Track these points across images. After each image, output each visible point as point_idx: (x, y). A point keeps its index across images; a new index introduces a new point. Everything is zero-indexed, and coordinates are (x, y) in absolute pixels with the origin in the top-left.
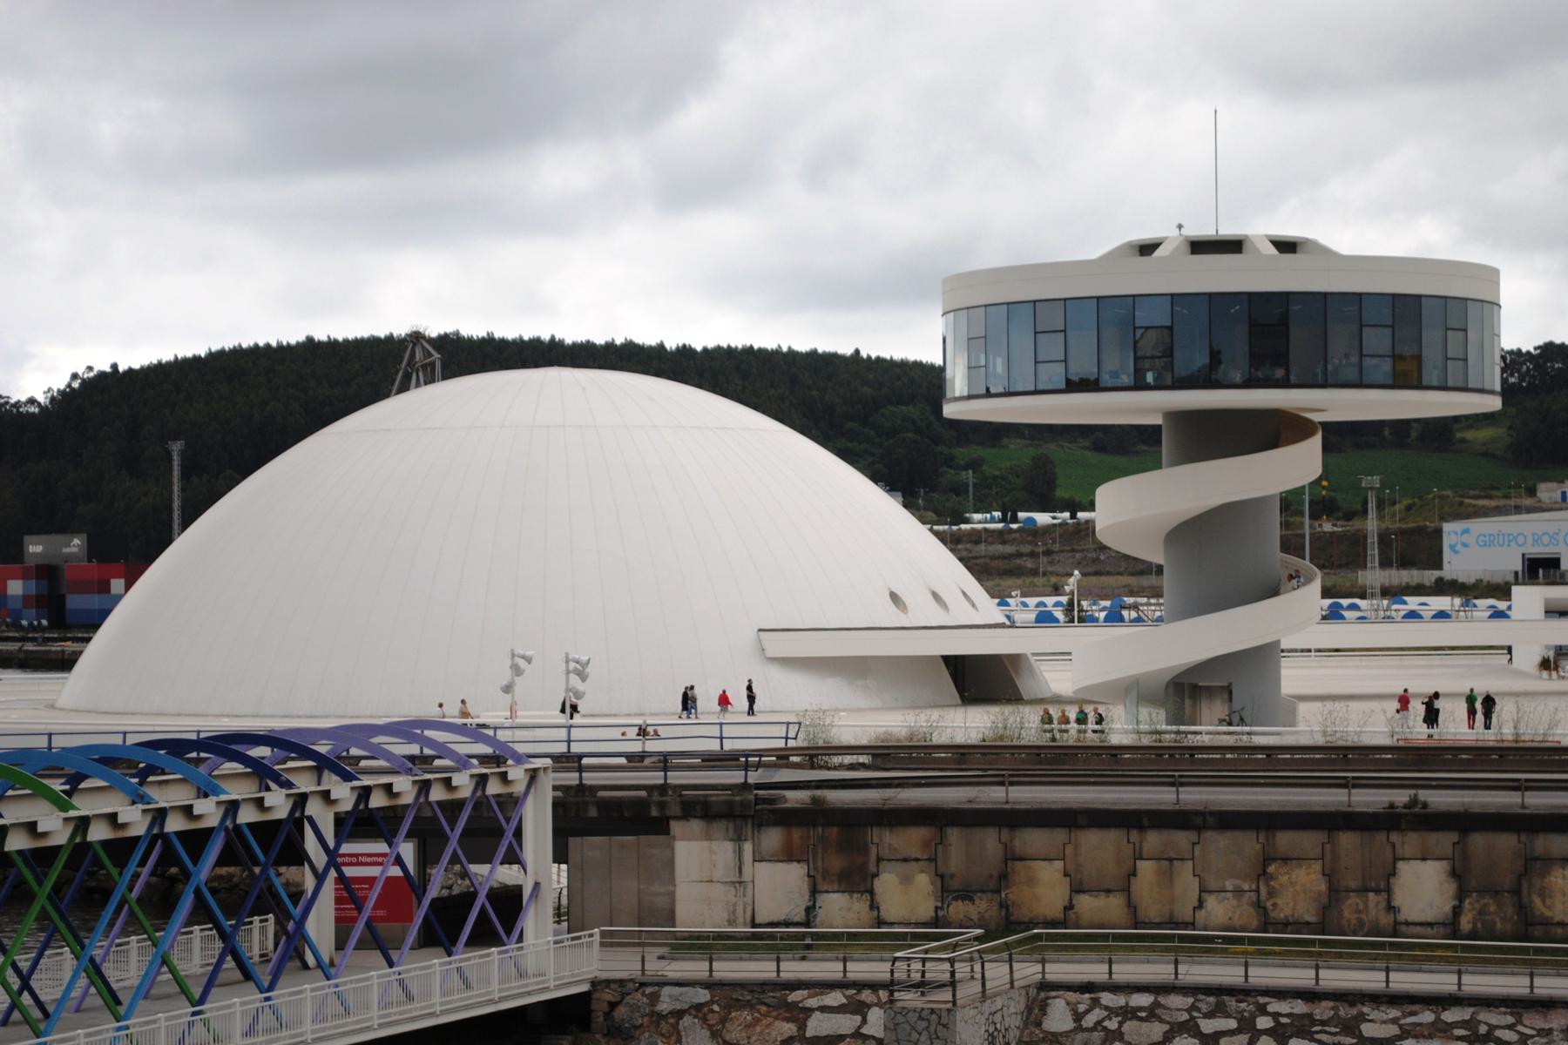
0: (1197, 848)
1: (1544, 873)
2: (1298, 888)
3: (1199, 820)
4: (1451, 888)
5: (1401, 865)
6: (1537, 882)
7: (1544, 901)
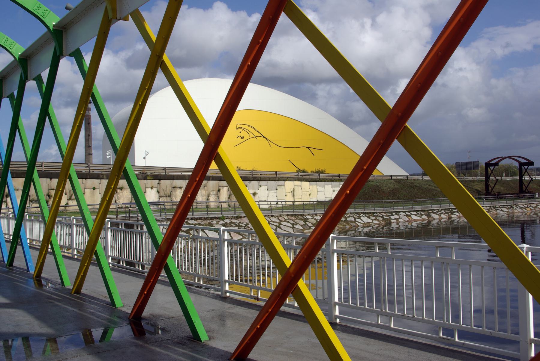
0: (100, 185)
1: (175, 192)
2: (124, 196)
3: (101, 176)
4: (157, 195)
5: (147, 189)
6: (174, 193)
7: (175, 198)
